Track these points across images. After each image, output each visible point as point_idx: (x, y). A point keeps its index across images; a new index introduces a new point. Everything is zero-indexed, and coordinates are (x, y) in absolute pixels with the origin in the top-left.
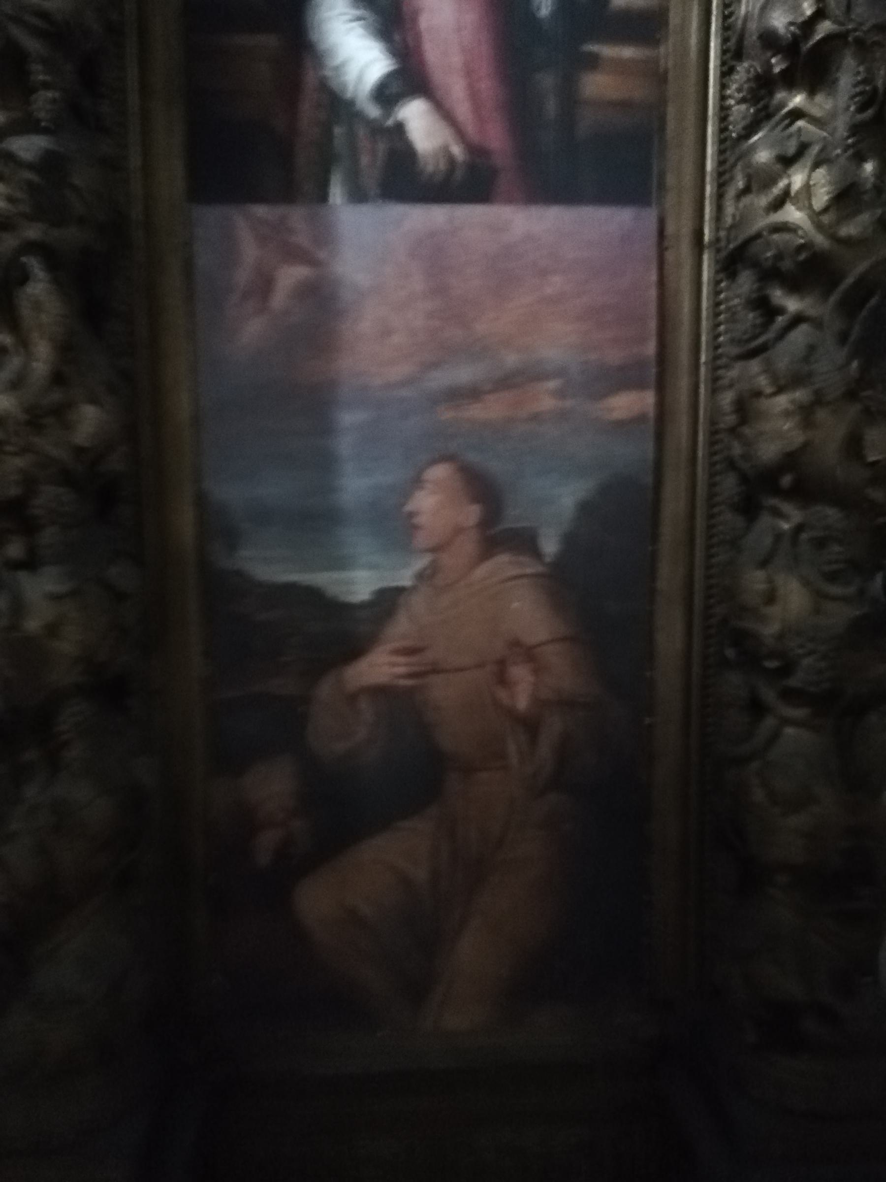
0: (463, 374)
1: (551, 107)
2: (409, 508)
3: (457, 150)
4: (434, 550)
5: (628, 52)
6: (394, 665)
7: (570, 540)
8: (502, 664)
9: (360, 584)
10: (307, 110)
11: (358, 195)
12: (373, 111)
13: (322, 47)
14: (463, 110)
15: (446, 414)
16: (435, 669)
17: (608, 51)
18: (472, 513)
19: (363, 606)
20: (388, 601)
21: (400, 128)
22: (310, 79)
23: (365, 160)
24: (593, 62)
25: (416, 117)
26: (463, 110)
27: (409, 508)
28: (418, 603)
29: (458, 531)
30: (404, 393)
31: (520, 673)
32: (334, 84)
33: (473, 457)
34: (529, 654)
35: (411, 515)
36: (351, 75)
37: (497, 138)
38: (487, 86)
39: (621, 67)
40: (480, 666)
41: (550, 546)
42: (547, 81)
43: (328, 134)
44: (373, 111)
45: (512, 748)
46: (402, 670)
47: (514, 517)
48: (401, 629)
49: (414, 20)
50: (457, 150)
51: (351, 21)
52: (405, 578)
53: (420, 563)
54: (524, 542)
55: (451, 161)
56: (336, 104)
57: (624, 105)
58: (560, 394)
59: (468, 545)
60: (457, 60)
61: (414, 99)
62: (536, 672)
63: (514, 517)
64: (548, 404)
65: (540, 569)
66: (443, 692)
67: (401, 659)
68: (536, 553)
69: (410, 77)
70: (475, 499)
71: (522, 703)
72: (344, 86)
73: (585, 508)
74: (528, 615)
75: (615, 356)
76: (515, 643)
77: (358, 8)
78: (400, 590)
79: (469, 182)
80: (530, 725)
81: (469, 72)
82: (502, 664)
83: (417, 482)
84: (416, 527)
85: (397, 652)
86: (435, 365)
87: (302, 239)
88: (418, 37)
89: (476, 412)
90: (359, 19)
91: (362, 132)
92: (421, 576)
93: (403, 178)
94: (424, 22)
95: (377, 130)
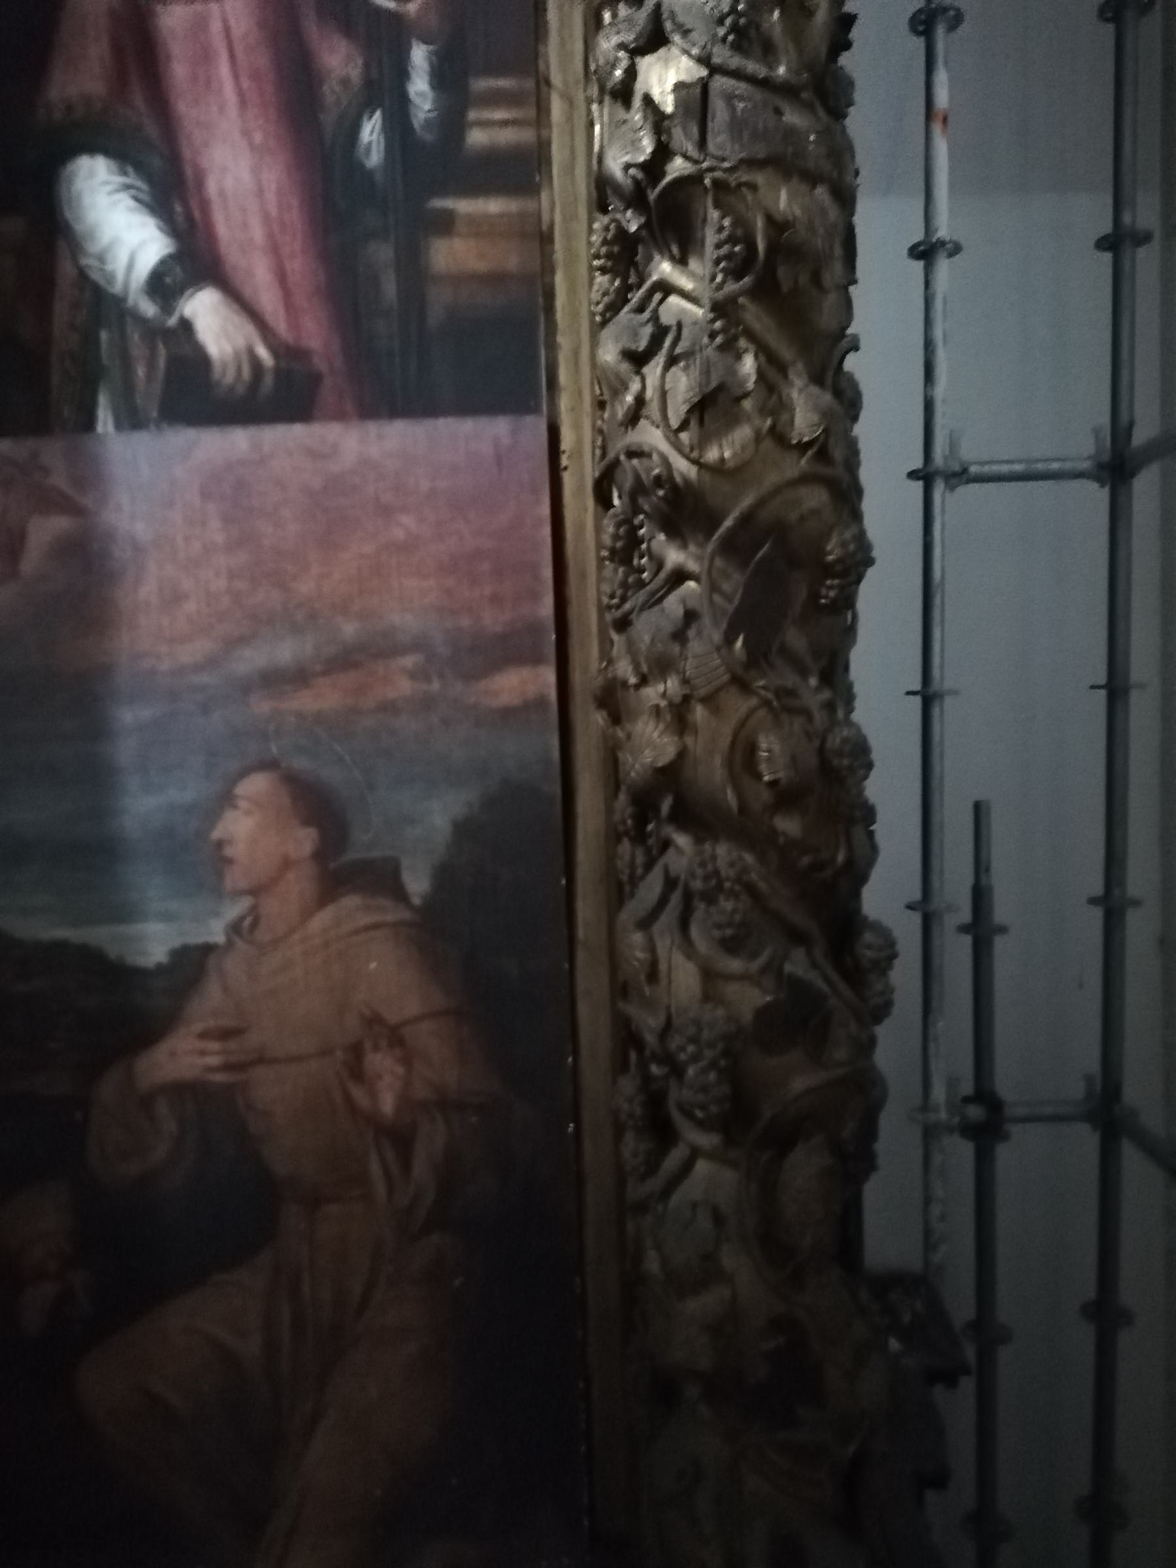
0: (285, 651)
1: (390, 288)
2: (216, 834)
3: (263, 352)
4: (255, 892)
5: (494, 206)
6: (203, 1053)
7: (444, 876)
8: (356, 1051)
9: (154, 942)
10: (61, 310)
11: (131, 419)
12: (149, 309)
13: (79, 228)
14: (269, 300)
15: (261, 706)
16: (261, 1059)
17: (464, 206)
18: (305, 840)
19: (160, 969)
20: (192, 963)
21: (186, 326)
22: (66, 269)
23: (141, 372)
24: (445, 224)
25: (204, 310)
26: (269, 300)
27: (216, 834)
28: (234, 966)
29: (287, 864)
30: (205, 678)
31: (383, 1064)
32: (95, 276)
33: (301, 763)
34: (396, 1038)
35: (220, 844)
36: (118, 264)
37: (315, 334)
38: (299, 265)
39: (481, 228)
40: (326, 1052)
41: (417, 885)
42: (382, 253)
43: (90, 339)
44: (149, 309)
45: (375, 1169)
46: (213, 1061)
47: (363, 844)
48: (210, 1003)
49: (200, 183)
50: (263, 352)
51: (117, 191)
52: (216, 932)
53: (234, 910)
54: (381, 879)
55: (256, 365)
56: (100, 302)
57: (495, 279)
58: (412, 675)
59: (299, 886)
60: (258, 233)
61: (201, 289)
62: (407, 1061)
63: (363, 844)
64: (404, 687)
65: (406, 915)
66: (273, 1091)
67: (215, 1046)
68: (399, 894)
69: (195, 259)
70: (307, 822)
71: (388, 1104)
72: (110, 278)
73: (463, 829)
74: (391, 980)
75: (493, 621)
76: (374, 1020)
77: (125, 173)
78: (207, 949)
79: (282, 394)
80: (400, 1138)
81: (274, 250)
82: (356, 1051)
83: (226, 799)
84: (230, 861)
85: (204, 1035)
86: (243, 640)
87: (59, 480)
88: (205, 205)
89: (306, 701)
90: (127, 187)
91: (135, 337)
92: (235, 928)
93: (193, 393)
94: (212, 187)
95: (153, 332)
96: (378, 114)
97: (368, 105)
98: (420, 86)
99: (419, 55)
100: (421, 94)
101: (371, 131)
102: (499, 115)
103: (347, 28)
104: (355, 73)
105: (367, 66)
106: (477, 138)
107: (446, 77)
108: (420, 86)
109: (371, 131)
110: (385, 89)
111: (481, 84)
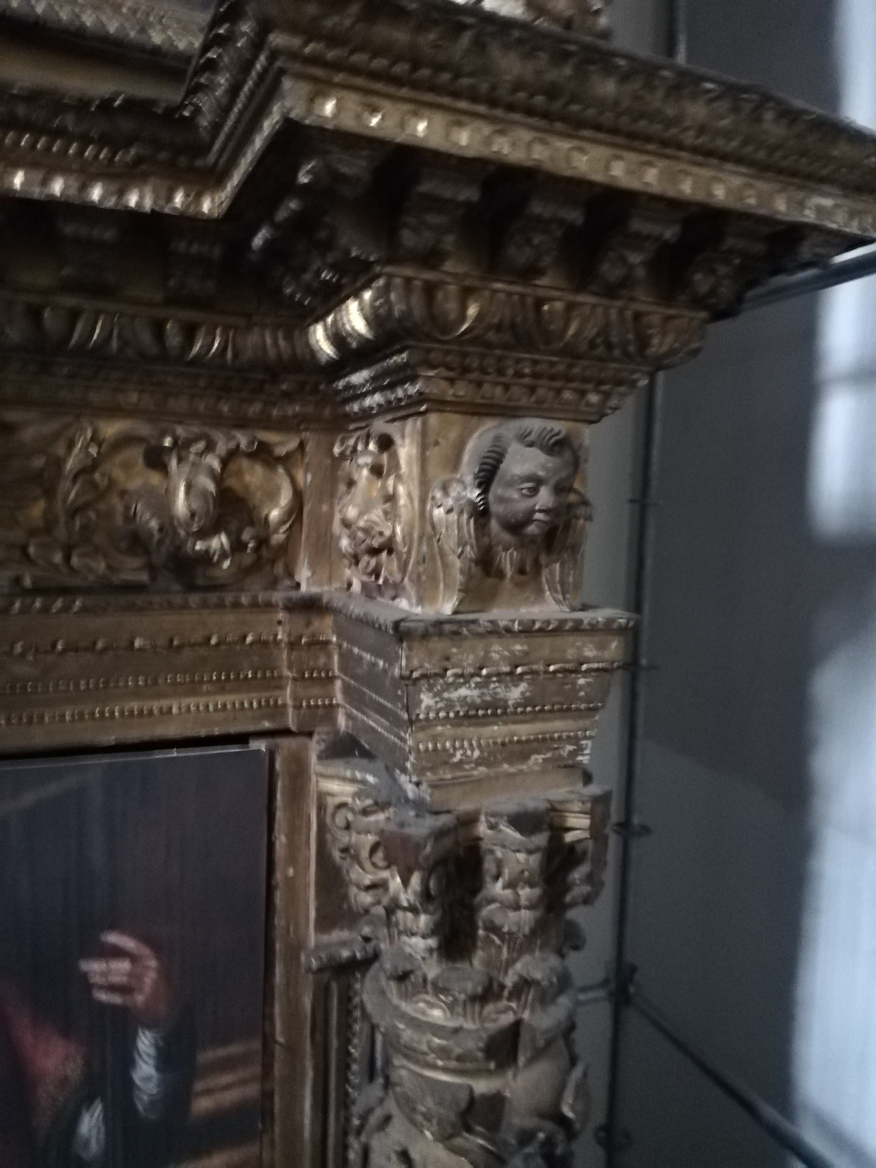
96: (98, 1109)
97: (88, 1102)
98: (146, 1071)
99: (145, 1042)
100: (148, 1079)
101: (90, 1124)
102: (226, 1078)
103: (66, 1032)
104: (74, 1070)
105: (87, 1063)
106: (203, 1105)
107: (175, 1059)
108: (146, 1071)
109: (90, 1124)
110: (107, 1078)
111: (207, 1056)
